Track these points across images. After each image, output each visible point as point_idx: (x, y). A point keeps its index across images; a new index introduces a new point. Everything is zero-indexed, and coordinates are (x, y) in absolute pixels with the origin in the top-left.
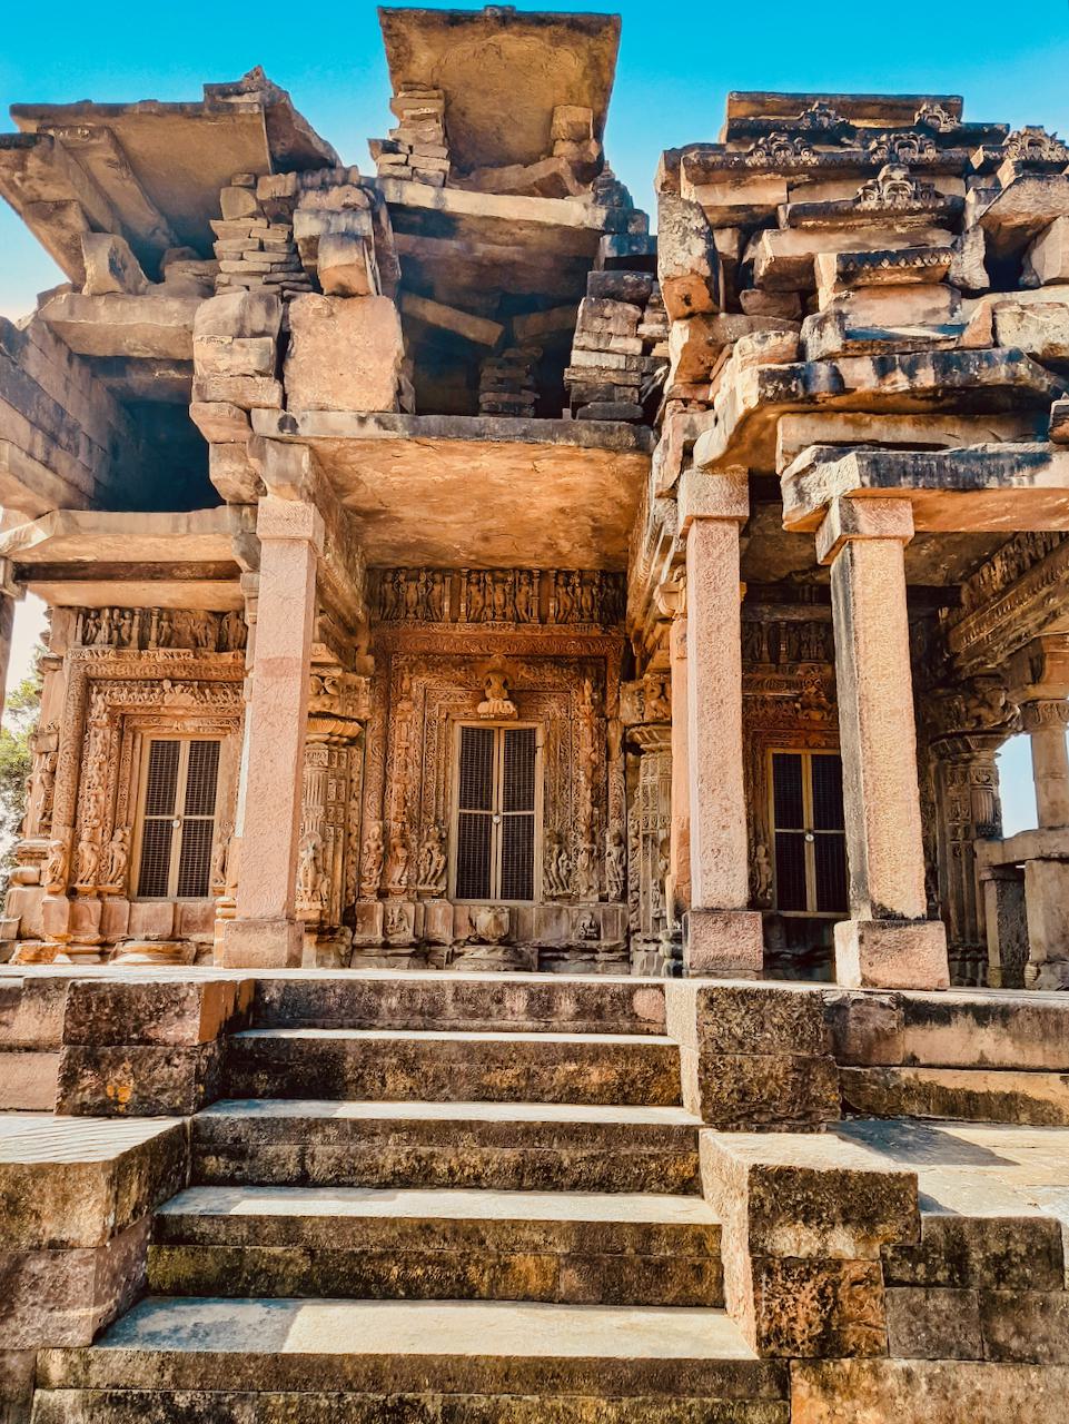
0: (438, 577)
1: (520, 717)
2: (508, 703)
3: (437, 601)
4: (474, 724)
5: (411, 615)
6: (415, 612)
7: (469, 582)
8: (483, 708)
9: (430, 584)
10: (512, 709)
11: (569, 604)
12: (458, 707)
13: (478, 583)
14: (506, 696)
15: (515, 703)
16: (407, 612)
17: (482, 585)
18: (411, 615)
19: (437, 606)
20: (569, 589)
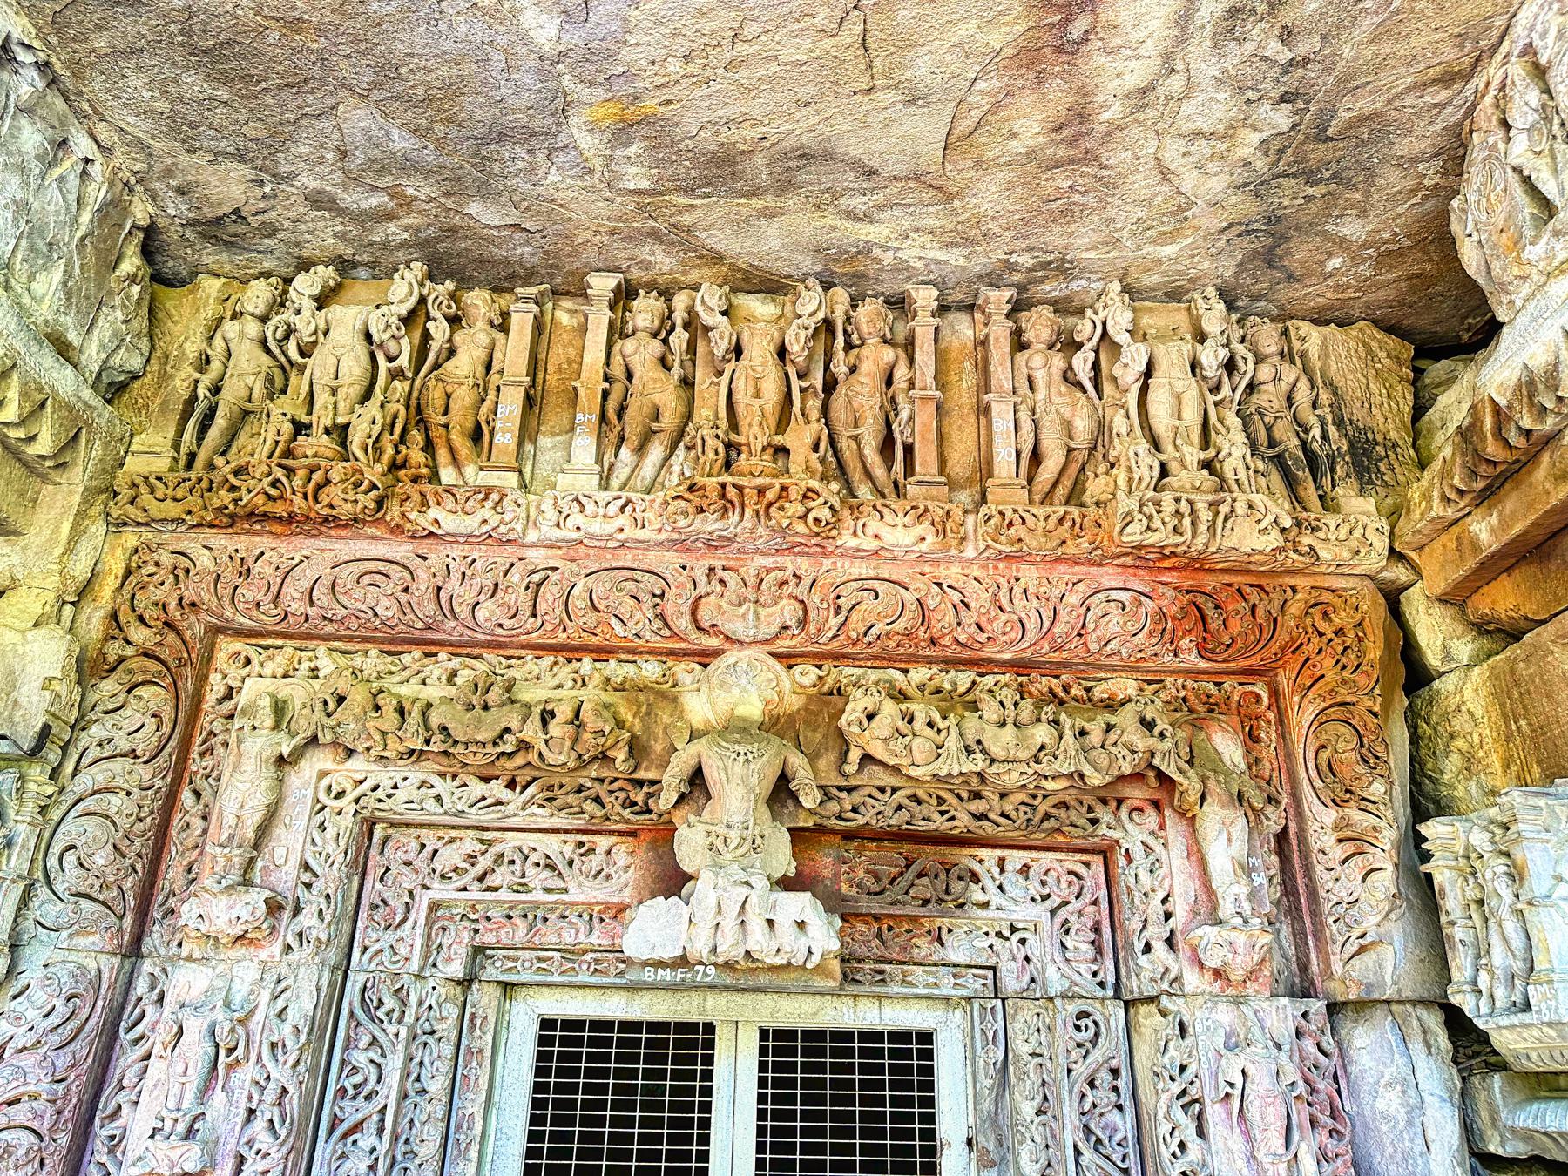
0: (478, 301)
1: (852, 971)
2: (801, 904)
3: (463, 397)
4: (616, 1007)
5: (317, 444)
6: (341, 432)
7: (617, 331)
8: (655, 930)
9: (439, 330)
10: (824, 936)
11: (1083, 427)
12: (535, 916)
13: (662, 331)
14: (784, 863)
15: (834, 903)
16: (300, 428)
17: (679, 339)
18: (317, 444)
19: (460, 418)
20: (1082, 363)
